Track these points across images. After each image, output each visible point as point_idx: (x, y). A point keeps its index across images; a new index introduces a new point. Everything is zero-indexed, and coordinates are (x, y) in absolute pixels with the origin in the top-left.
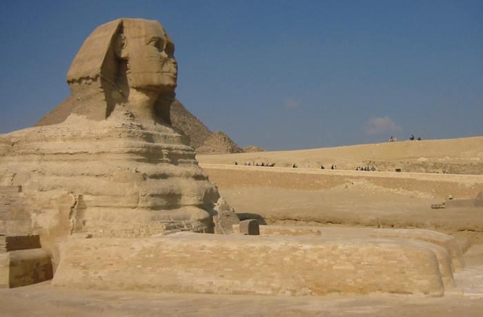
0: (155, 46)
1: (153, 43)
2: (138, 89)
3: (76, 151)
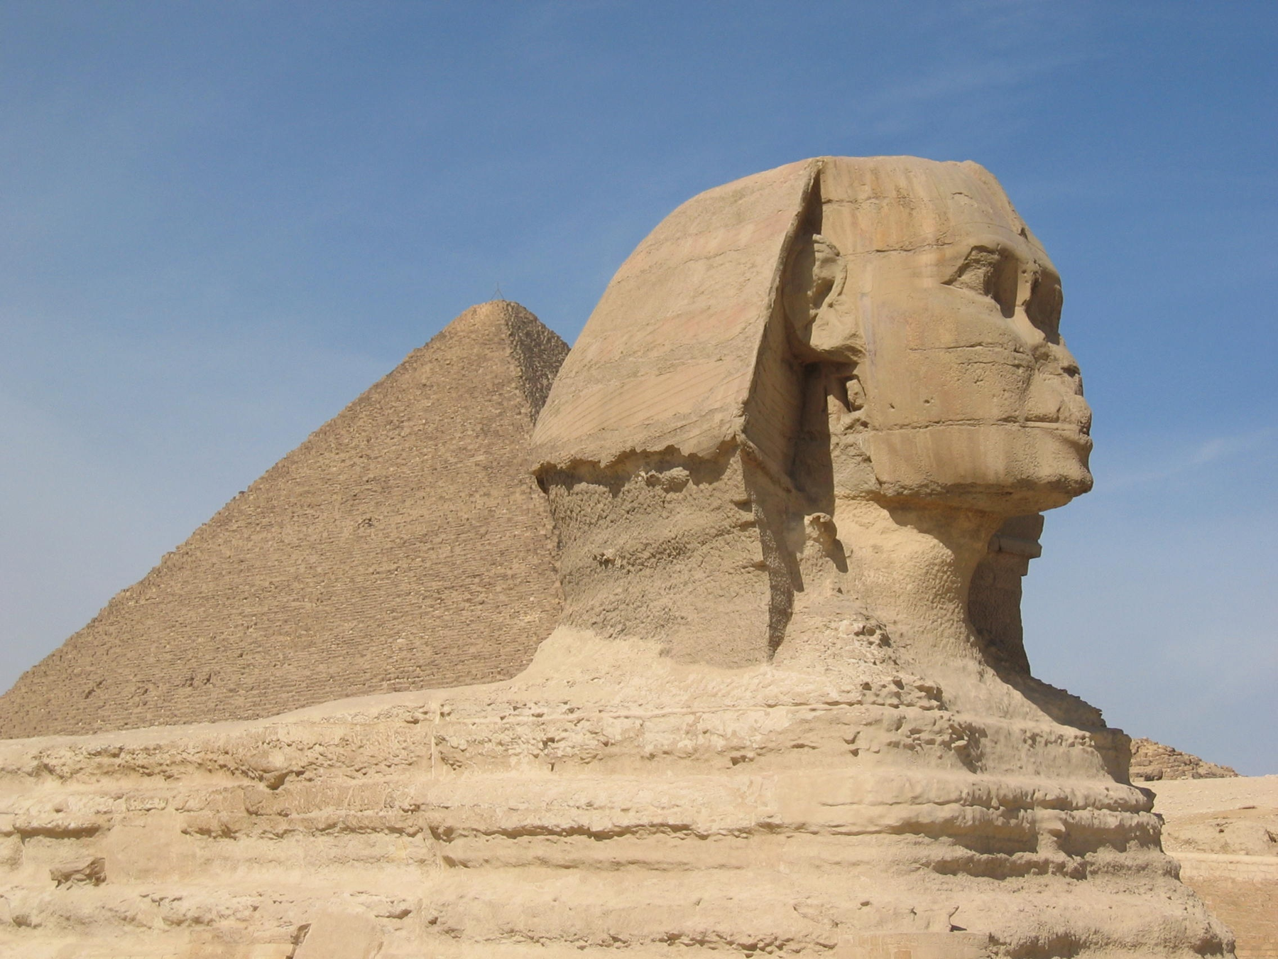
0: (986, 293)
1: (981, 272)
2: (904, 506)
3: (626, 821)
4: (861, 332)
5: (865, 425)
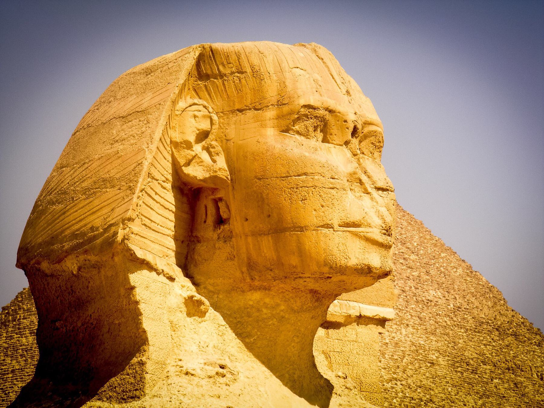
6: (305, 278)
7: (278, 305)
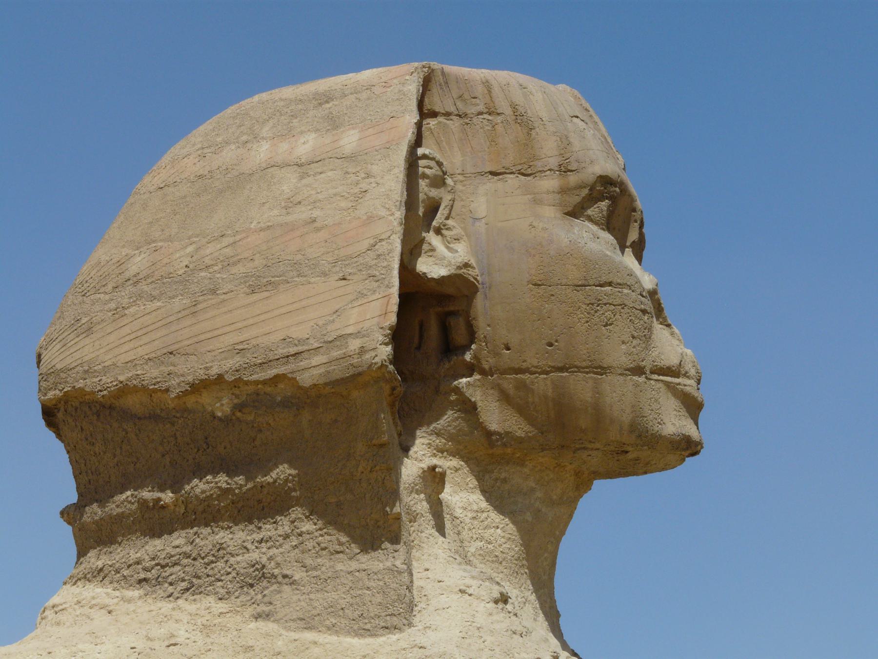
4: (473, 262)
5: (470, 369)
6: (592, 449)
7: (533, 490)
